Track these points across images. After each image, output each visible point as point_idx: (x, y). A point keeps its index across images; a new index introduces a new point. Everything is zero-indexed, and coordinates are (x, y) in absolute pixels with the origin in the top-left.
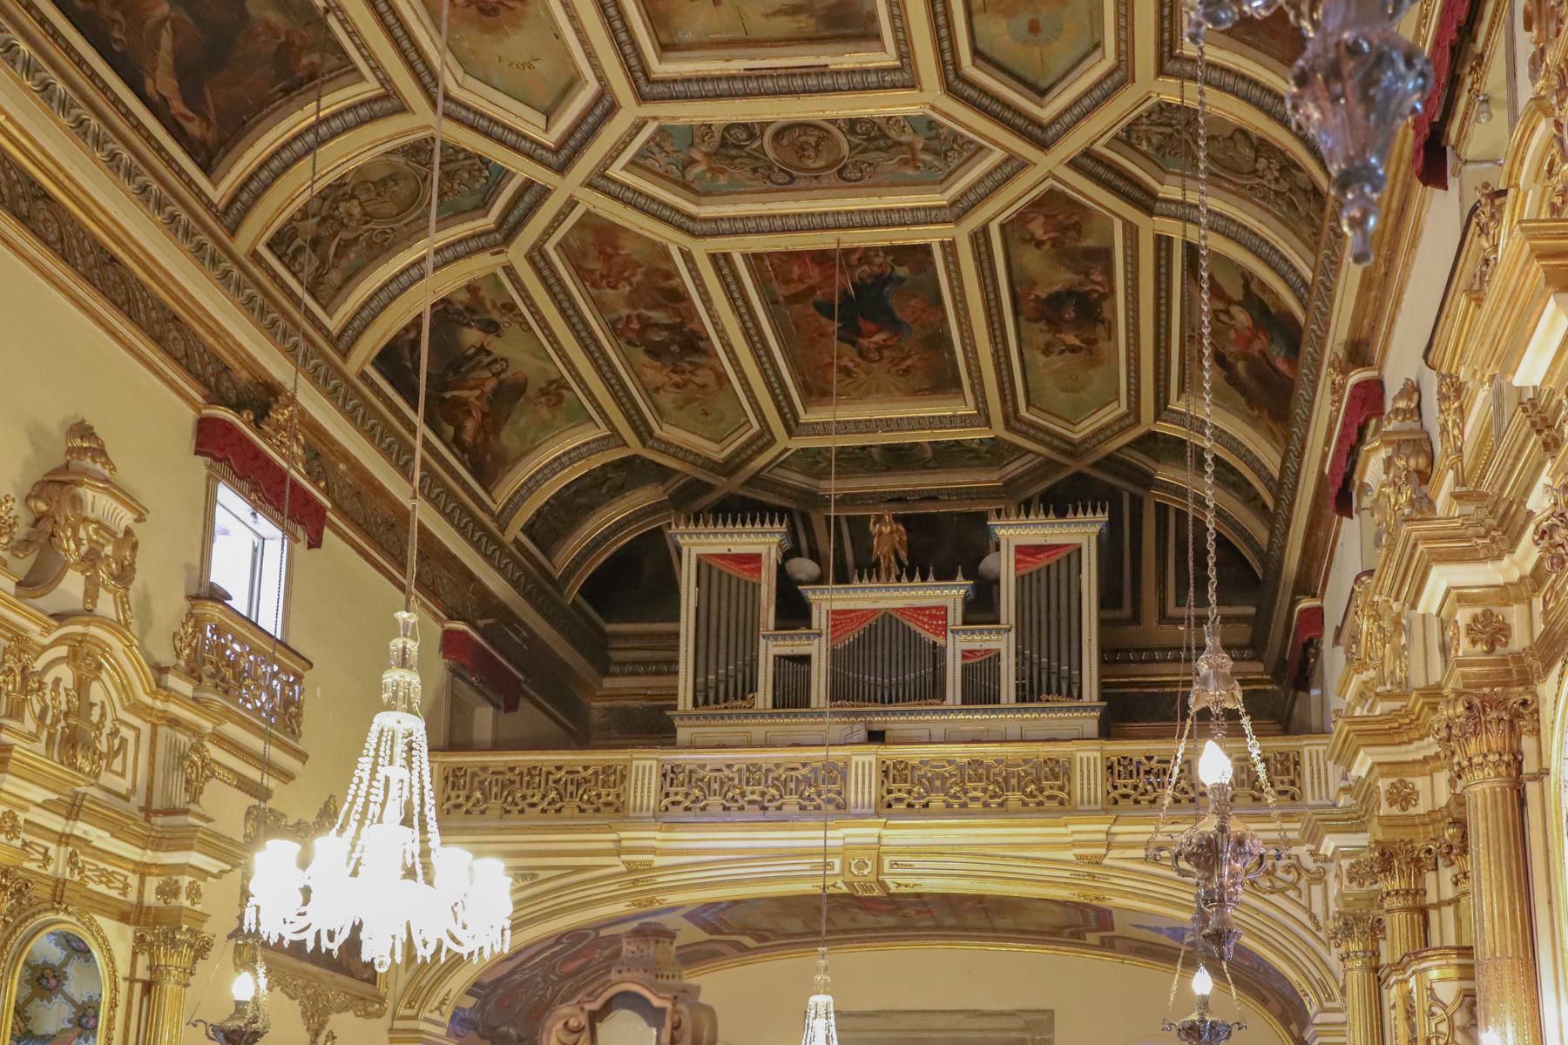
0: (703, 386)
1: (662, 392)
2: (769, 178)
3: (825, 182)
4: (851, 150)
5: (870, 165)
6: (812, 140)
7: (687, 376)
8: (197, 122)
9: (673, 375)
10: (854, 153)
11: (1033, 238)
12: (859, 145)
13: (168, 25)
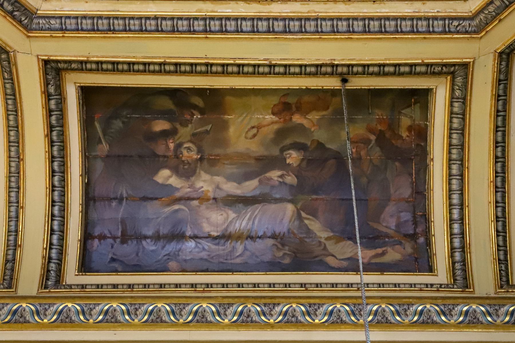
8: (389, 249)
13: (303, 215)
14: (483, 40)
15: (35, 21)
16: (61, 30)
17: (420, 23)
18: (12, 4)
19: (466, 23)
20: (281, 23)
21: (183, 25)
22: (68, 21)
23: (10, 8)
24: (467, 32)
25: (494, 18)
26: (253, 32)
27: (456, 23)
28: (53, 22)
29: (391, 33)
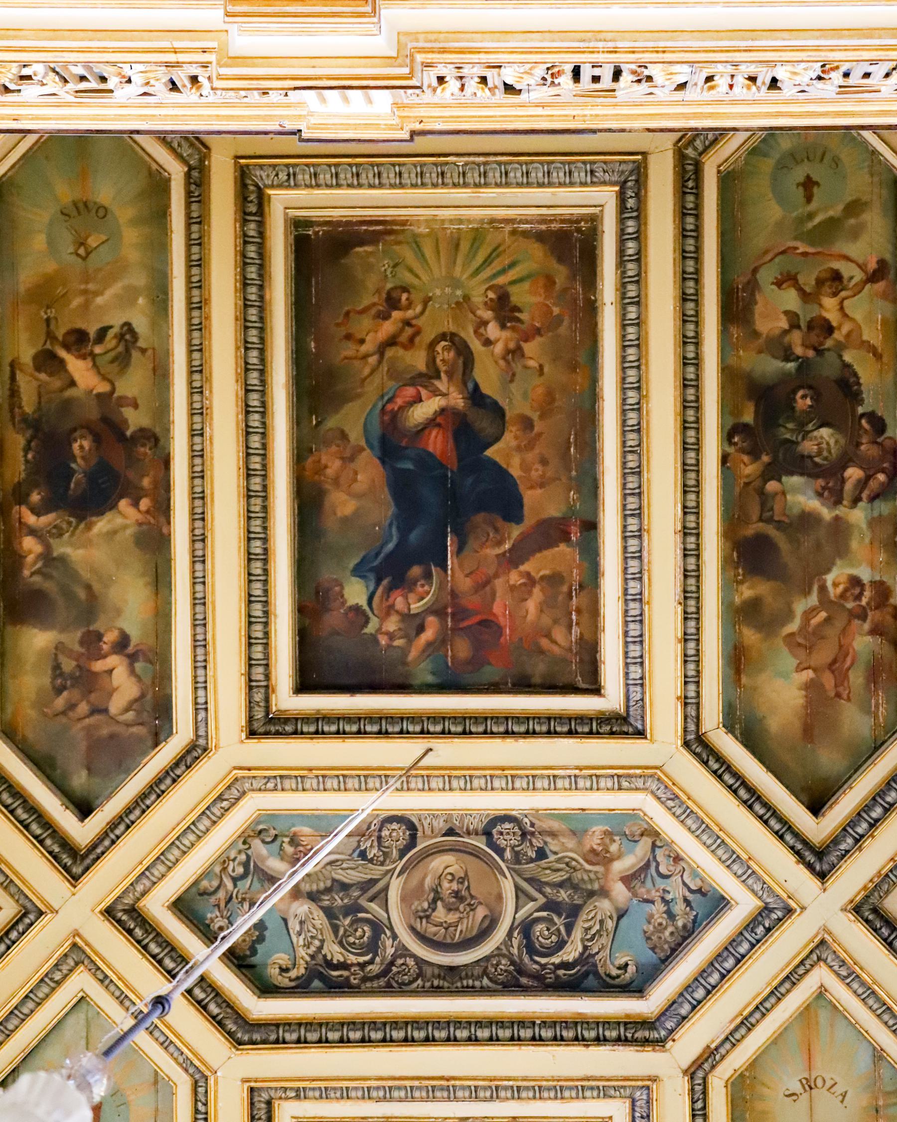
0: (787, 279)
1: (872, 265)
2: (524, 834)
3: (440, 825)
4: (386, 889)
5: (363, 855)
6: (440, 914)
7: (806, 314)
9: (833, 317)
10: (381, 885)
11: (132, 658)
12: (371, 900)
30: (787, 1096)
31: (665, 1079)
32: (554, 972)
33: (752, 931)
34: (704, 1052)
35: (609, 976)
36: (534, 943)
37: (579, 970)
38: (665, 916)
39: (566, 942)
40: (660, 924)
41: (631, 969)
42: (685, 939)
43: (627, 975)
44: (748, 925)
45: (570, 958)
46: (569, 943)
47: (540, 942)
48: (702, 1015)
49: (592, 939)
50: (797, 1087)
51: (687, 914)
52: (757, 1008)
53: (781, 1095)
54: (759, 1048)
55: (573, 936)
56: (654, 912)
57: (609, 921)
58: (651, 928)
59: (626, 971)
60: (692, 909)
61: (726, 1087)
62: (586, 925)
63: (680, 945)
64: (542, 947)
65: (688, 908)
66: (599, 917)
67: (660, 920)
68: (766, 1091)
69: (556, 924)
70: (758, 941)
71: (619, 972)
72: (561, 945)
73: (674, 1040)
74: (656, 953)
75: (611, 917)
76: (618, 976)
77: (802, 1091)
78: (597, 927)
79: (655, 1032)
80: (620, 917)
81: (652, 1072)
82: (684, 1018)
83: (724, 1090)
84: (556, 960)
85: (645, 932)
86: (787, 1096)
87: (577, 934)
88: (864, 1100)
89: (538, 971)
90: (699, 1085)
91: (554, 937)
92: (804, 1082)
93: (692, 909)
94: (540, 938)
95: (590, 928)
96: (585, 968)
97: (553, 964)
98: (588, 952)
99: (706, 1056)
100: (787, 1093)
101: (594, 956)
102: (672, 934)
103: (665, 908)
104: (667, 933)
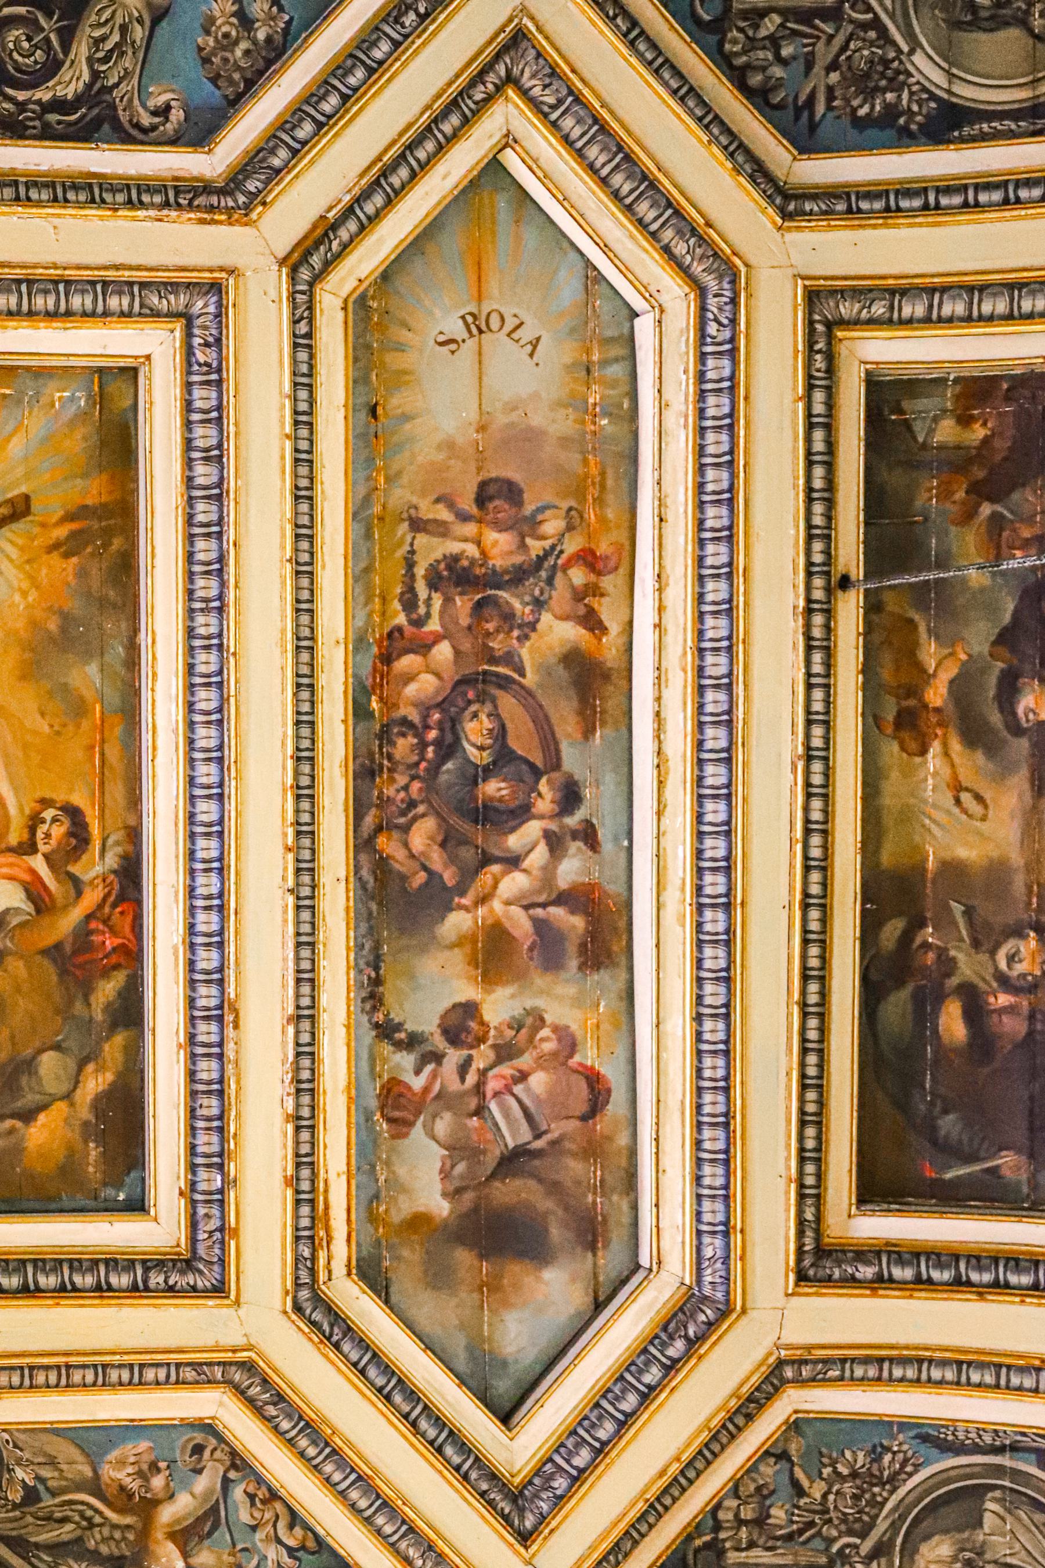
14: (752, 261)
15: (707, 1291)
16: (726, 1234)
17: (711, 412)
18: (671, 1338)
19: (712, 302)
20: (710, 732)
21: (714, 957)
22: (707, 1217)
23: (680, 1345)
24: (734, 301)
25: (702, 240)
26: (729, 797)
27: (712, 329)
28: (708, 1252)
29: (733, 476)
30: (441, 344)
31: (248, 274)
32: (40, 117)
33: (396, 21)
34: (315, 226)
35: (137, 126)
36: (5, 63)
37: (84, 116)
38: (234, 20)
39: (63, 63)
40: (226, 36)
41: (177, 115)
42: (269, 63)
43: (168, 125)
44: (389, 15)
45: (69, 92)
46: (68, 64)
47: (15, 62)
48: (312, 162)
49: (106, 60)
50: (455, 328)
51: (273, 19)
52: (402, 156)
53: (432, 343)
54: (402, 241)
55: (72, 56)
56: (217, 14)
57: (138, 28)
58: (211, 42)
59: (167, 119)
60: (281, 9)
61: (345, 309)
62: (97, 34)
63: (261, 73)
64: (18, 70)
65: (275, 9)
66: (119, 20)
67: (225, 29)
68: (405, 335)
69: (43, 30)
70: (406, 37)
71: (157, 120)
72: (52, 68)
73: (264, 204)
74: (218, 88)
75: (140, 21)
76: (154, 128)
77: (466, 335)
78: (116, 38)
79: (229, 199)
80: (156, 21)
81: (228, 261)
82: (278, 171)
83: (340, 315)
84: (43, 95)
85: (200, 49)
86: (441, 344)
87: (81, 49)
88: (569, 352)
89: (11, 114)
90: (303, 293)
91: (39, 52)
92: (470, 319)
93: (281, 9)
94: (15, 55)
95: (104, 39)
96: (95, 111)
97: (39, 102)
98: (98, 85)
99: (319, 231)
100: (441, 338)
101: (110, 89)
102: (247, 53)
103: (235, 8)
104: (239, 53)
